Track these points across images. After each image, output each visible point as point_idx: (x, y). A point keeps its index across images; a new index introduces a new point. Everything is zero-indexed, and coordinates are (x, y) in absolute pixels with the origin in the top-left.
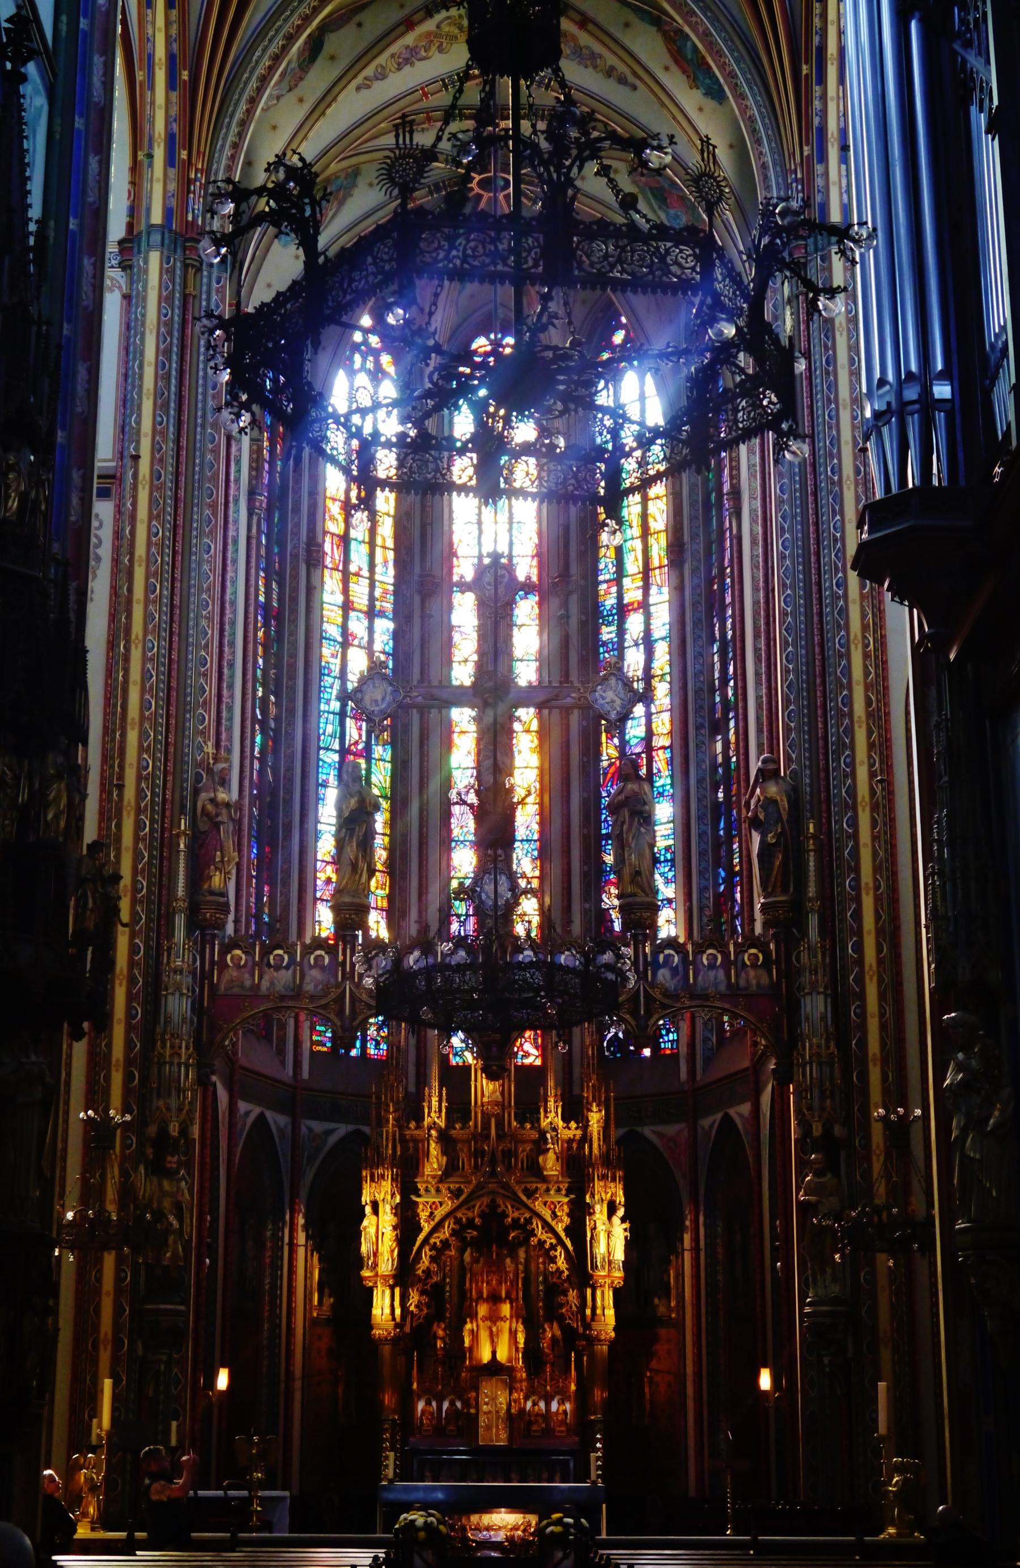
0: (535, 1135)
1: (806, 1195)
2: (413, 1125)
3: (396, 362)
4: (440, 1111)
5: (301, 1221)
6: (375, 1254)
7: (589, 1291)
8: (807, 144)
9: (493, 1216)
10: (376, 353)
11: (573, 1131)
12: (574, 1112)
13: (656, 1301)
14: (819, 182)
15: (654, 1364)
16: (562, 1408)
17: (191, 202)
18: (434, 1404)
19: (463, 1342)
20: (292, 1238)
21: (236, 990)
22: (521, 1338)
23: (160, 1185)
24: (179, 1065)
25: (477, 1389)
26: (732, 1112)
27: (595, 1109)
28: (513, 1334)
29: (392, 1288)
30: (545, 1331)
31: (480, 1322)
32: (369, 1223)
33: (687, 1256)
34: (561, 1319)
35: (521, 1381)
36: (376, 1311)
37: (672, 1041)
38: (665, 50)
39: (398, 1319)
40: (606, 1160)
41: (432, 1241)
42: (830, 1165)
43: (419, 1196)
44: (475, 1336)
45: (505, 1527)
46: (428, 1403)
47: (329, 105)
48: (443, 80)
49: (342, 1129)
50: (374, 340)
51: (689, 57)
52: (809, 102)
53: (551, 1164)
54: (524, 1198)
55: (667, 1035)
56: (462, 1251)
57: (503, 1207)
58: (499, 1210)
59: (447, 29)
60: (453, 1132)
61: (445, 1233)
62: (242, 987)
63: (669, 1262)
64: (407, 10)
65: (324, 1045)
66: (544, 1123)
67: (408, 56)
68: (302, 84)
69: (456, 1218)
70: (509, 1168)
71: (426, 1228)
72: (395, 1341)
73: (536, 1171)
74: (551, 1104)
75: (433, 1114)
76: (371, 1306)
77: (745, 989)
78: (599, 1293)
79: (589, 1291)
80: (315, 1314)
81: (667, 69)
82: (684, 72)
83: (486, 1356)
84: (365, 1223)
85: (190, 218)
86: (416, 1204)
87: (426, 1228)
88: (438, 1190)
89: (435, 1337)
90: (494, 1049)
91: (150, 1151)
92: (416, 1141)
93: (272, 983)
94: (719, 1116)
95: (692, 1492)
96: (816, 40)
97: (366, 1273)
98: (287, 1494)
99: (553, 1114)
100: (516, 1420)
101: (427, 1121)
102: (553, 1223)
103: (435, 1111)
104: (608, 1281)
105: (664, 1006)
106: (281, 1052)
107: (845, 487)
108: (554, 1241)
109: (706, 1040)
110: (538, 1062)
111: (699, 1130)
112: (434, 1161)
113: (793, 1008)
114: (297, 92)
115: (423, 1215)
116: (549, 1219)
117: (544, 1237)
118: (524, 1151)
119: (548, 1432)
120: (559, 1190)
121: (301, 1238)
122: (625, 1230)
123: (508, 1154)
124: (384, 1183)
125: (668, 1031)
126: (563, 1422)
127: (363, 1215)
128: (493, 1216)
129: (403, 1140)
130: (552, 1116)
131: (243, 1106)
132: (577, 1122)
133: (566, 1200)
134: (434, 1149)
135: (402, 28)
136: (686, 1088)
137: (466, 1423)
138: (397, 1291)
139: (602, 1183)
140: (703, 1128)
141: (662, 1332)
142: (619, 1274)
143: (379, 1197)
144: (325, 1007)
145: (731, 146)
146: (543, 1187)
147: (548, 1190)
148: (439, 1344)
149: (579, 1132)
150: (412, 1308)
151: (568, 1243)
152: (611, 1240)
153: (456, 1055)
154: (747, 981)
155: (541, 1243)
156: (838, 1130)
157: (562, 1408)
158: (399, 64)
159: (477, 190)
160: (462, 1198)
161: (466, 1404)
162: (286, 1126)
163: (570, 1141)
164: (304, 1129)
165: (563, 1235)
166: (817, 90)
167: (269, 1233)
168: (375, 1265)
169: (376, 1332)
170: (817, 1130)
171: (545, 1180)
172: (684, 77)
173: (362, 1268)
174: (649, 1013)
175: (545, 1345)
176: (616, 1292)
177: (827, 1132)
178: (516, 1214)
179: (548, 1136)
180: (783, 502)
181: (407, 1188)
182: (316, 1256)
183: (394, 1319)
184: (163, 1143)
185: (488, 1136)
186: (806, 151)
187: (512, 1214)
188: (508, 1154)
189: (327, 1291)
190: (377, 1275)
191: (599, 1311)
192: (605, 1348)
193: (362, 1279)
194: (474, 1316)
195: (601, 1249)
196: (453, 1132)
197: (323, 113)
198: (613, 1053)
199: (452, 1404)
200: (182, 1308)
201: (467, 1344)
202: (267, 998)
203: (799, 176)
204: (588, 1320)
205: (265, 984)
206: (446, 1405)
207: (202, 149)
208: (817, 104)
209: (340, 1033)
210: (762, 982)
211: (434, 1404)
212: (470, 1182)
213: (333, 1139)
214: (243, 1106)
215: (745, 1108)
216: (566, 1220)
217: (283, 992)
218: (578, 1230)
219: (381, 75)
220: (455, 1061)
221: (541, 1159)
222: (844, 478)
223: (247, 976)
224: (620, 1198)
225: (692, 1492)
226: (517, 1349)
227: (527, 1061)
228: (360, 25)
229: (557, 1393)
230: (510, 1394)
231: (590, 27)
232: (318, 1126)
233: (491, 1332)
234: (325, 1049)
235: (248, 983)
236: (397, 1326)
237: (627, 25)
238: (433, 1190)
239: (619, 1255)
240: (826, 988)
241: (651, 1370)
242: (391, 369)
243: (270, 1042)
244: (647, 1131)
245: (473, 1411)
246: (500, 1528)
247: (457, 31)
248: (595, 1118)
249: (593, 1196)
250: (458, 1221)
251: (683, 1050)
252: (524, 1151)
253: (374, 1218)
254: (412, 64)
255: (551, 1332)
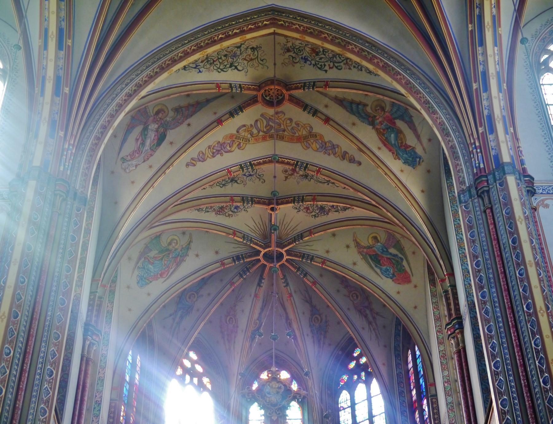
3: (211, 383)
8: (481, 126)
10: (200, 376)
14: (492, 144)
17: (63, 160)
38: (377, 138)
47: (168, 168)
48: (241, 165)
50: (199, 368)
51: (393, 142)
52: (479, 102)
59: (243, 134)
64: (218, 116)
67: (219, 149)
68: (151, 159)
81: (379, 148)
82: (390, 150)
85: (62, 168)
96: (481, 68)
107: (539, 315)
114: (148, 163)
135: (215, 124)
145: (423, 191)
158: (213, 153)
159: (263, 261)
166: (484, 95)
172: (391, 154)
180: (491, 337)
186: (481, 130)
197: (164, 172)
203: (477, 144)
207: (75, 133)
208: (485, 103)
219: (202, 158)
222: (538, 309)
228: (189, 125)
231: (331, 122)
237: (354, 124)
242: (209, 386)
247: (249, 136)
254: (222, 155)
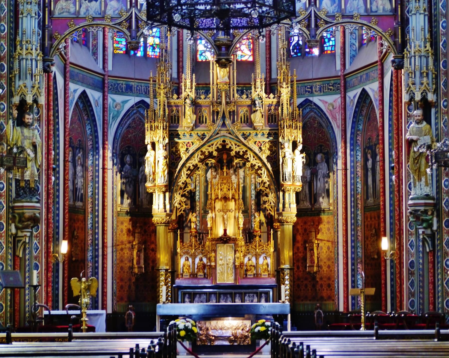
0: (249, 102)
1: (410, 135)
2: (175, 96)
4: (192, 88)
5: (109, 154)
6: (154, 174)
7: (281, 194)
9: (224, 150)
11: (272, 100)
12: (271, 87)
13: (321, 199)
15: (319, 236)
16: (265, 262)
18: (190, 260)
19: (207, 225)
20: (104, 165)
21: (65, 15)
22: (241, 221)
23: (22, 132)
24: (31, 60)
25: (215, 251)
26: (367, 88)
27: (284, 85)
28: (237, 219)
29: (164, 193)
30: (255, 217)
31: (217, 213)
32: (150, 155)
33: (340, 174)
34: (265, 210)
35: (241, 247)
36: (155, 207)
37: (332, 46)
39: (168, 212)
40: (292, 117)
41: (188, 165)
42: (427, 118)
43: (180, 139)
44: (214, 220)
45: (231, 328)
46: (187, 260)
49: (133, 100)
53: (258, 119)
54: (242, 140)
55: (329, 42)
56: (207, 171)
57: (230, 145)
58: (228, 147)
60: (199, 101)
61: (195, 161)
62: (69, 12)
63: (329, 177)
65: (121, 50)
66: (254, 95)
69: (202, 151)
70: (233, 122)
71: (184, 157)
72: (167, 224)
73: (249, 122)
74: (258, 84)
75: (187, 90)
76: (152, 204)
77: (376, 12)
78: (287, 195)
79: (281, 194)
80: (119, 210)
83: (220, 233)
84: (148, 155)
86: (177, 143)
87: (184, 157)
88: (191, 135)
89: (190, 221)
90: (223, 49)
91: (15, 113)
92: (177, 106)
93: (87, 10)
94: (359, 91)
95: (341, 309)
97: (148, 184)
98: (104, 312)
99: (260, 89)
100: (238, 269)
101: (184, 95)
102: (260, 154)
103: (188, 89)
104: (293, 188)
105: (327, 22)
106: (95, 54)
108: (260, 165)
109: (352, 45)
110: (251, 59)
111: (347, 99)
112: (188, 119)
113: (405, 22)
115: (182, 150)
116: (257, 152)
117: (254, 162)
118: (242, 111)
119: (257, 276)
120: (263, 134)
121: (109, 164)
122: (303, 158)
123: (232, 114)
124: (158, 131)
125: (329, 40)
126: (266, 270)
127: (146, 151)
128: (224, 150)
129: (169, 106)
130: (259, 91)
131: (72, 86)
132: (274, 94)
133: (267, 140)
134: (189, 110)
136: (339, 74)
137: (209, 271)
138: (167, 194)
139: (289, 130)
140: (350, 98)
141: (324, 217)
142: (299, 184)
143: (155, 140)
144: (120, 24)
146: (253, 133)
147: (257, 135)
148: (193, 225)
149: (275, 100)
150: (176, 205)
151: (269, 165)
152: (294, 163)
153: (201, 55)
154: (377, 7)
155: (253, 166)
156: (431, 97)
157: (265, 262)
160: (205, 140)
161: (209, 259)
162: (99, 98)
163: (270, 106)
164: (110, 101)
165: (265, 161)
167: (90, 162)
168: (154, 180)
169: (155, 219)
170: (418, 97)
171: (255, 129)
173: (145, 182)
174: (317, 27)
175: (256, 225)
176: (297, 194)
177: (424, 99)
178: (238, 149)
179: (257, 102)
181: (173, 135)
182: (119, 175)
183: (165, 211)
184: (23, 107)
185: (220, 103)
187: (235, 149)
188: (232, 114)
189: (126, 196)
190: (155, 186)
191: (287, 205)
192: (291, 227)
193: (145, 188)
194: (213, 209)
195: (287, 170)
196: (199, 101)
198: (296, 53)
199: (201, 260)
200: (38, 205)
201: (209, 225)
202: (84, 19)
204: (281, 211)
205: (83, 10)
206: (197, 260)
209: (129, 40)
210: (386, 7)
211: (190, 260)
212: (210, 130)
213: (127, 106)
214: (72, 86)
215: (375, 85)
216: (268, 153)
217: (95, 16)
218: (275, 159)
220: (200, 59)
221: (252, 116)
223: (72, 5)
224: (300, 139)
225: (341, 309)
226: (239, 228)
227: (244, 59)
229: (263, 253)
230: (235, 254)
232: (119, 98)
233: (223, 218)
234: (122, 52)
235: (72, 10)
236: (167, 215)
238: (188, 135)
239: (299, 173)
240: (425, 10)
241: (318, 240)
243: (89, 48)
244: (316, 100)
245: (213, 264)
246: (228, 328)
248: (285, 92)
249: (283, 138)
250: (203, 153)
251: (338, 51)
252: (242, 111)
253: (153, 151)
255: (260, 217)
